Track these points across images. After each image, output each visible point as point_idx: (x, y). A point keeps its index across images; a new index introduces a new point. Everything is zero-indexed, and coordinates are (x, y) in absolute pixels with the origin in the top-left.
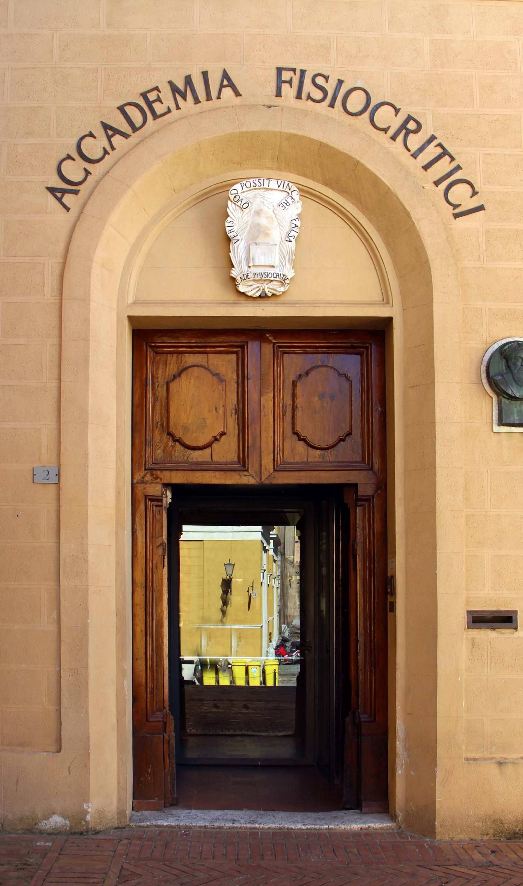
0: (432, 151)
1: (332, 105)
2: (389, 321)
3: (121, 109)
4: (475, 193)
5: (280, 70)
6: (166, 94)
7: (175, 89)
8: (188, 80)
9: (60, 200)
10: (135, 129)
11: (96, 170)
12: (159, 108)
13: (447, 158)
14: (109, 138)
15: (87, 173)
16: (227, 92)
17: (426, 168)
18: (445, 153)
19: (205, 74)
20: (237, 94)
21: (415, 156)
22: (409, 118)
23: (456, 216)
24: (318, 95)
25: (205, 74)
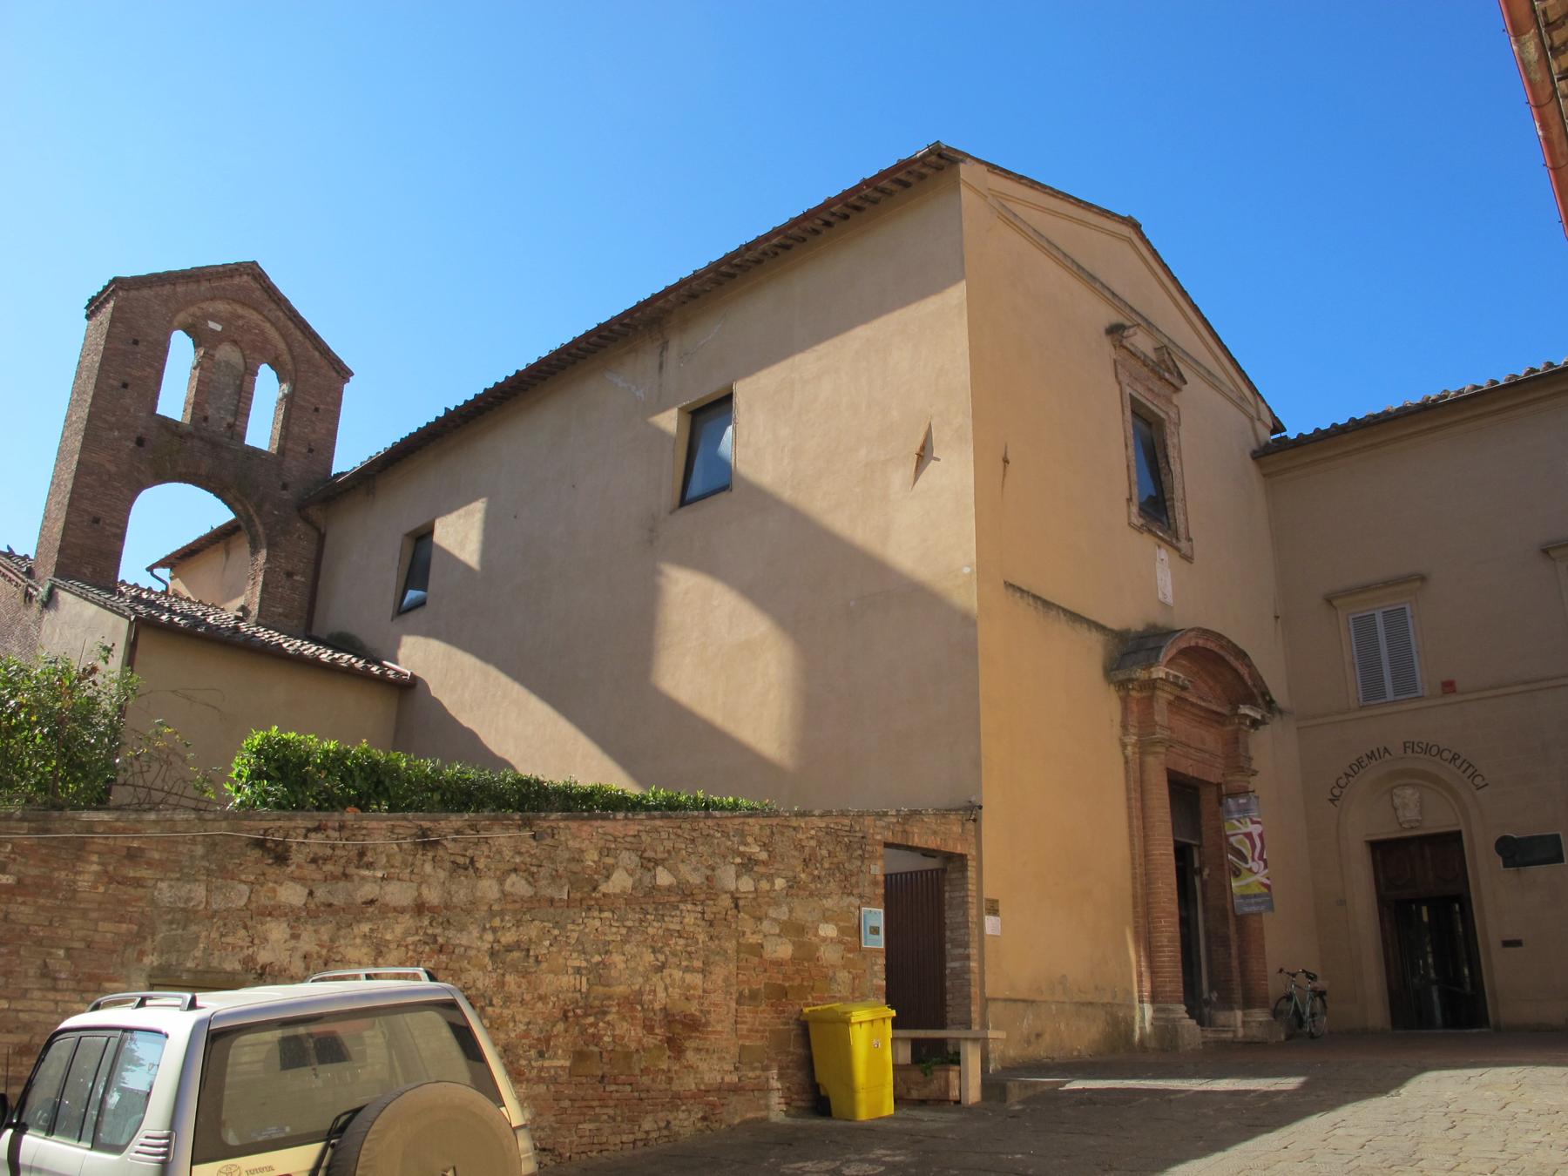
0: (1465, 765)
1: (1425, 753)
3: (1350, 766)
4: (1484, 779)
5: (1405, 743)
6: (1365, 759)
8: (1372, 752)
9: (1333, 803)
10: (1356, 774)
12: (1363, 764)
13: (1471, 768)
14: (1347, 778)
15: (1342, 792)
16: (1387, 754)
17: (1464, 772)
18: (1470, 765)
19: (1378, 749)
20: (1390, 754)
21: (1459, 768)
22: (1455, 754)
23: (1478, 789)
24: (1419, 750)
25: (1378, 749)
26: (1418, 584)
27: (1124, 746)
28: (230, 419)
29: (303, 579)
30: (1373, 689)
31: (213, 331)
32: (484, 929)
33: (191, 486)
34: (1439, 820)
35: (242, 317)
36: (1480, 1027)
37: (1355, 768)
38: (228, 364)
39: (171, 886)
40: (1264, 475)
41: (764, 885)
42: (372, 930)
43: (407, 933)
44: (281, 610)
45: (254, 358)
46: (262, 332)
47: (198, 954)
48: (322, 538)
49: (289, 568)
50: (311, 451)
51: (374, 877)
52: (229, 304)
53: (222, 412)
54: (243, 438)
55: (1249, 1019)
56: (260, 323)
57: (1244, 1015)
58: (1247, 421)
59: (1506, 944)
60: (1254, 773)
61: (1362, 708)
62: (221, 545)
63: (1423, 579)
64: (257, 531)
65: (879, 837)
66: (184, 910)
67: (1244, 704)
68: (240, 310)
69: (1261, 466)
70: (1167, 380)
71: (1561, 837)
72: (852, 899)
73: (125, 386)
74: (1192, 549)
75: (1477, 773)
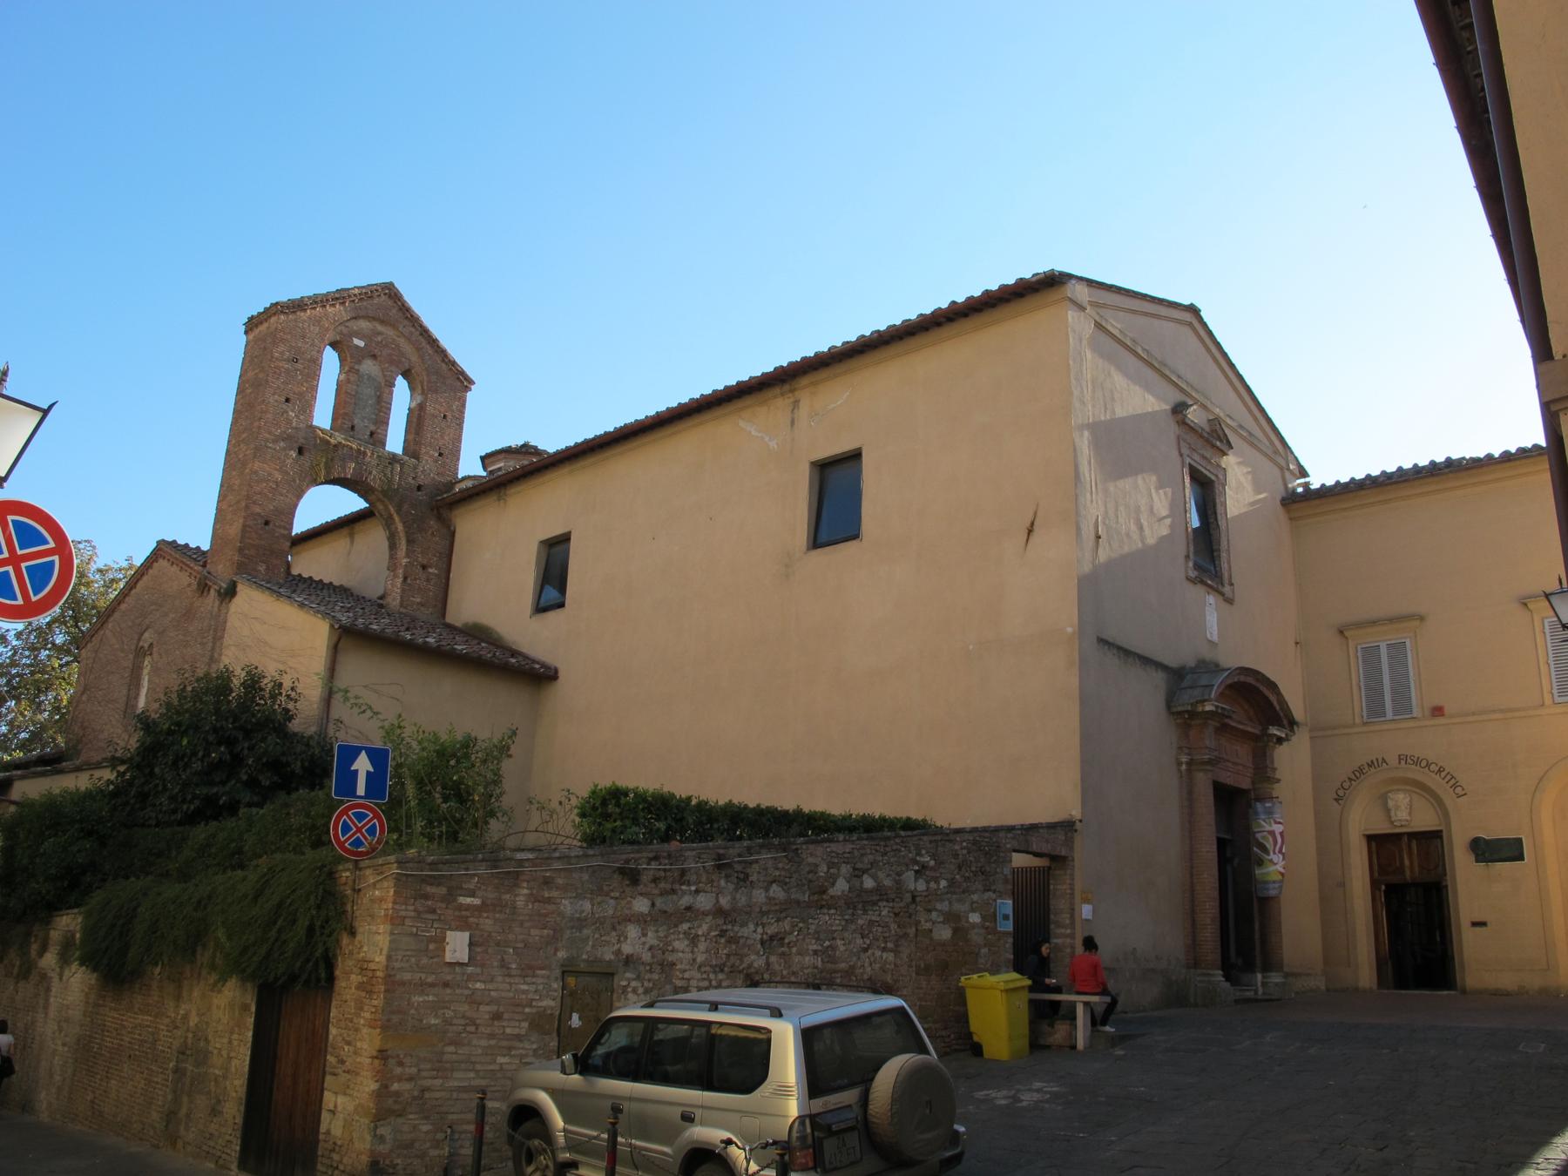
0: (1449, 777)
2: (1441, 831)
3: (1353, 772)
4: (1463, 789)
5: (1399, 756)
7: (1368, 764)
8: (1372, 762)
11: (1347, 792)
12: (1364, 771)
15: (1345, 793)
16: (1384, 764)
17: (1447, 782)
21: (1443, 779)
22: (1441, 767)
25: (1377, 760)
26: (1418, 623)
27: (1179, 764)
28: (373, 428)
29: (436, 571)
30: (1376, 709)
31: (357, 347)
32: (757, 925)
33: (338, 487)
34: (1424, 820)
35: (380, 333)
36: (1449, 989)
37: (1358, 775)
38: (370, 377)
39: (571, 903)
40: (1291, 519)
41: (933, 885)
42: (689, 928)
43: (710, 930)
44: (418, 600)
45: (392, 371)
46: (398, 346)
47: (589, 948)
48: (453, 534)
49: (425, 562)
50: (440, 455)
51: (691, 891)
52: (369, 321)
53: (366, 421)
54: (384, 444)
55: (1269, 980)
56: (395, 337)
57: (1264, 977)
58: (1276, 471)
59: (1475, 924)
60: (1278, 781)
61: (1365, 724)
62: (345, 531)
63: (1422, 618)
64: (397, 528)
65: (1008, 846)
66: (579, 919)
67: (1273, 725)
68: (380, 328)
69: (1288, 512)
70: (1218, 448)
71: (1524, 840)
72: (990, 893)
73: (287, 400)
74: (1233, 592)
75: (1458, 784)
